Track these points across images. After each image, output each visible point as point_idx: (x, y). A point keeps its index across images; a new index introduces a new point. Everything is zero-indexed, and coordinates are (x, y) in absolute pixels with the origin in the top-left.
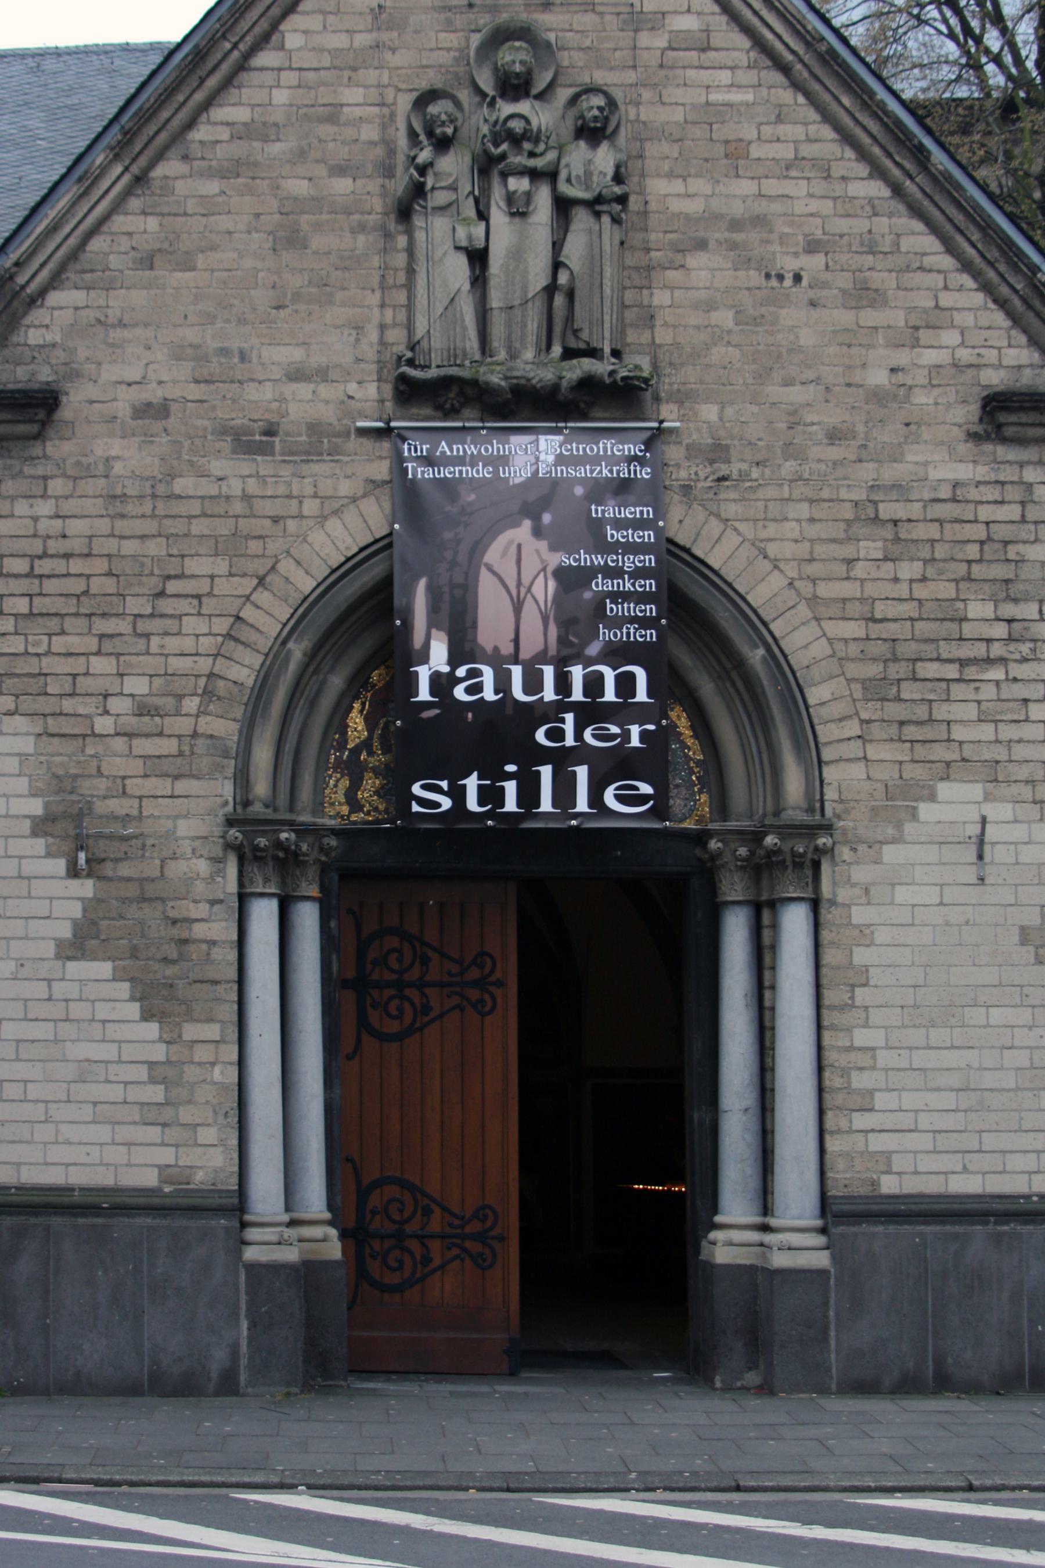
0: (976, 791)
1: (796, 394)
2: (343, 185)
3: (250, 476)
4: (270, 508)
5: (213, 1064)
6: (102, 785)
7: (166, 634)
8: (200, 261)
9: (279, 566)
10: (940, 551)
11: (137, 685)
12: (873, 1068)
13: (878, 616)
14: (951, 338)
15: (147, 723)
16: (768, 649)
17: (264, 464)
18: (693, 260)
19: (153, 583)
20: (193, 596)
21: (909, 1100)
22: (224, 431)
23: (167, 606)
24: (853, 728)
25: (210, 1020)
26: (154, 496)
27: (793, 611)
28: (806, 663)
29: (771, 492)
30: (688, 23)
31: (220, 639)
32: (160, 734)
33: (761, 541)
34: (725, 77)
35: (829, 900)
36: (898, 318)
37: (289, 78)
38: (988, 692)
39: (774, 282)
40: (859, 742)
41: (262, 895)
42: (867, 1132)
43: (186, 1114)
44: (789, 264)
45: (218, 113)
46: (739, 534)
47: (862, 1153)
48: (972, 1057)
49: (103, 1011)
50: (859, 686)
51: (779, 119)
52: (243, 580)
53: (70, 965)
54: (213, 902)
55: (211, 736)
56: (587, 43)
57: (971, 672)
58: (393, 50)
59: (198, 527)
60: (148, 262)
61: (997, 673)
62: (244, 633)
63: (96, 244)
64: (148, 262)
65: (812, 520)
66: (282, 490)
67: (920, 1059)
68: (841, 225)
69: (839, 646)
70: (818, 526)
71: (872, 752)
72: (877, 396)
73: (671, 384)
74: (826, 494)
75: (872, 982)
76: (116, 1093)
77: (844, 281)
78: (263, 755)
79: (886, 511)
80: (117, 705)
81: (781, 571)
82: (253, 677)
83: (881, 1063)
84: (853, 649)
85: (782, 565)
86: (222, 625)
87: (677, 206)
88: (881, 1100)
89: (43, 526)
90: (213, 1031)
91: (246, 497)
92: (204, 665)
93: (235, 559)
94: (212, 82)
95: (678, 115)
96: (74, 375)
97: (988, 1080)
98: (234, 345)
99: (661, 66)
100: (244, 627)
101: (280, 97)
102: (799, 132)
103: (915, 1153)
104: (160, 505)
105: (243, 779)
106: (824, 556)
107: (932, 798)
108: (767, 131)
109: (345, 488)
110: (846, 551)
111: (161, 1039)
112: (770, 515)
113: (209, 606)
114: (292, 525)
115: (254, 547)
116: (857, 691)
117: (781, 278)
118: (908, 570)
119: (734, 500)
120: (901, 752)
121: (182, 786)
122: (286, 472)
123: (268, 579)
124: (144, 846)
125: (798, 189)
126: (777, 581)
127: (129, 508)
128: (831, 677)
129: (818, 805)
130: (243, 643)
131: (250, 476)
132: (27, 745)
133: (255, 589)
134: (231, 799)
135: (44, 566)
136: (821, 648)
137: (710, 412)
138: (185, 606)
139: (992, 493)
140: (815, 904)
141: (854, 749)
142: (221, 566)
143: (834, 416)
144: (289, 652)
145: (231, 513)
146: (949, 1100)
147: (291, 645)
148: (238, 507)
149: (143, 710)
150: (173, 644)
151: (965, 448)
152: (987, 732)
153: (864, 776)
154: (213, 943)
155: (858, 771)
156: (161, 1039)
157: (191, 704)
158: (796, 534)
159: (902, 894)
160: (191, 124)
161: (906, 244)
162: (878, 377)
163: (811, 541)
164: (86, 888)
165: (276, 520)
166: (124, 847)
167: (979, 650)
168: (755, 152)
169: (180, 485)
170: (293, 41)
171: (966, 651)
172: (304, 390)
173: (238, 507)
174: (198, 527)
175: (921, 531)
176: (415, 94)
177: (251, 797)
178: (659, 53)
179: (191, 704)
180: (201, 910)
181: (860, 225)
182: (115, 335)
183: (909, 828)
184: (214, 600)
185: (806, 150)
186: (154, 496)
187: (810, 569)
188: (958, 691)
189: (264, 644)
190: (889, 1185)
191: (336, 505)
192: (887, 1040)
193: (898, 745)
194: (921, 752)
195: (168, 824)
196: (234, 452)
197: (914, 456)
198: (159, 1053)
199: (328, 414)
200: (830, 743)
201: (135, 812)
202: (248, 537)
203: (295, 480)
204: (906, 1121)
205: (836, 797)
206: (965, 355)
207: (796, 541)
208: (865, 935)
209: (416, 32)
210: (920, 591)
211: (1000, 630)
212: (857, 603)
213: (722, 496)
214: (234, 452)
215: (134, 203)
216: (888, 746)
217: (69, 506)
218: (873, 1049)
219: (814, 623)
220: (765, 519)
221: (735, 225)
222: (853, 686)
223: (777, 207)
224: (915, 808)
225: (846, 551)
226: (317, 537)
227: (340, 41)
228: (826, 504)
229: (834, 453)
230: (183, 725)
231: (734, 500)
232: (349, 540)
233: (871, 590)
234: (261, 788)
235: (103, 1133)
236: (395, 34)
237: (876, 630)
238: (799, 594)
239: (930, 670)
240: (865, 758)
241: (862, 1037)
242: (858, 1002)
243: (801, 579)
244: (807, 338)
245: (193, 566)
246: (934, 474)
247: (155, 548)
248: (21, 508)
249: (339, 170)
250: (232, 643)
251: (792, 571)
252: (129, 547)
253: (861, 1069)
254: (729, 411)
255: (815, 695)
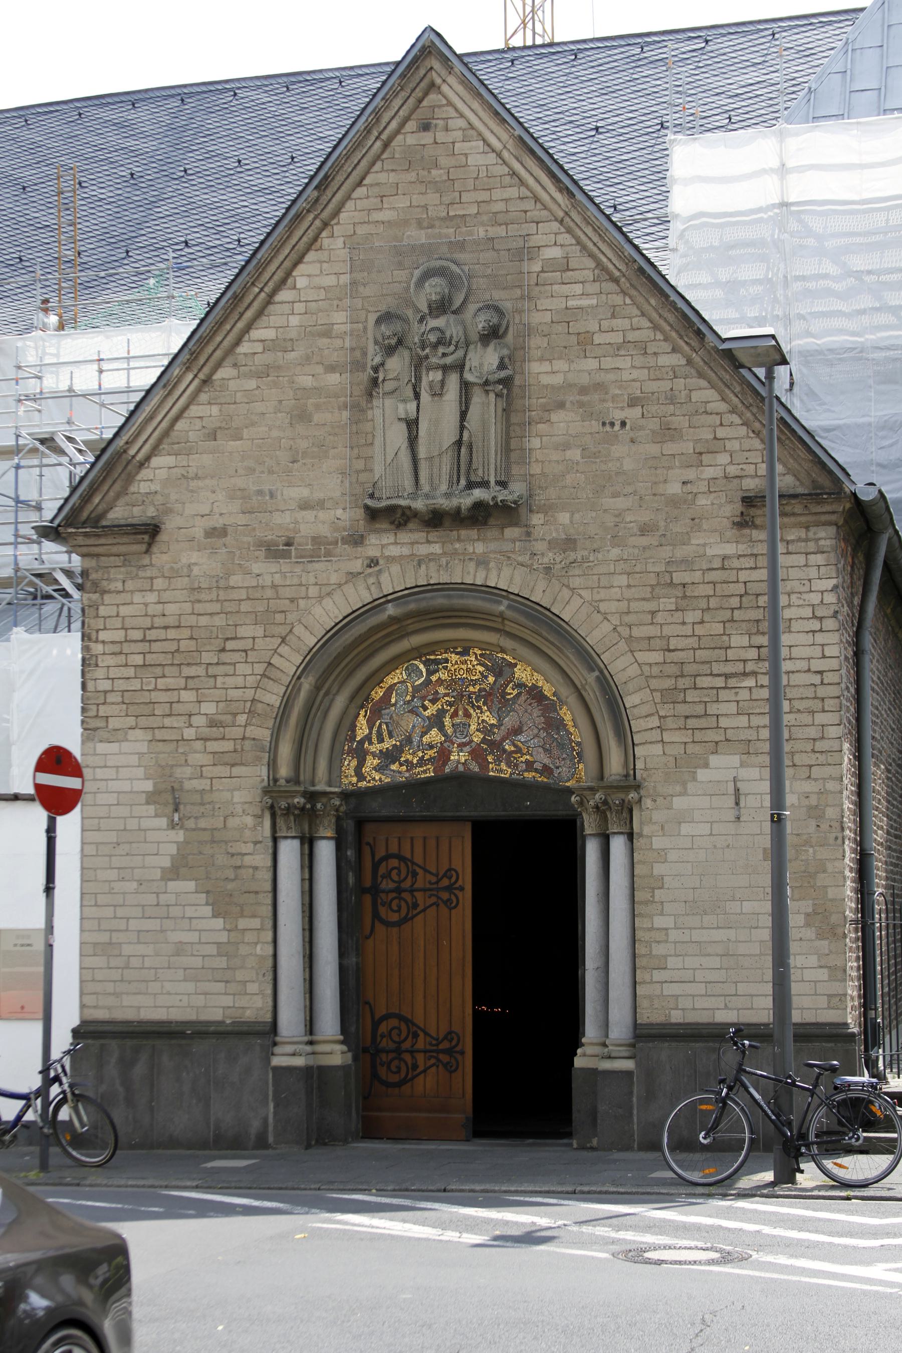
0: (735, 760)
1: (621, 503)
2: (334, 379)
3: (276, 573)
4: (287, 593)
5: (256, 944)
6: (188, 771)
7: (226, 675)
8: (245, 433)
9: (295, 630)
10: (713, 603)
11: (209, 708)
12: (666, 941)
13: (671, 647)
14: (723, 459)
15: (215, 732)
16: (601, 672)
17: (284, 565)
18: (554, 417)
19: (218, 643)
20: (242, 651)
21: (690, 962)
22: (260, 544)
23: (226, 657)
24: (654, 722)
25: (254, 916)
26: (218, 587)
27: (616, 647)
28: (624, 680)
29: (602, 569)
30: (555, 253)
31: (259, 677)
32: (223, 738)
33: (596, 601)
34: (578, 289)
35: (638, 833)
36: (688, 447)
37: (299, 307)
38: (744, 695)
39: (608, 428)
40: (659, 731)
41: (286, 838)
42: (662, 983)
43: (240, 975)
44: (618, 415)
45: (255, 334)
46: (581, 597)
47: (658, 996)
48: (731, 934)
49: (190, 912)
50: (659, 694)
51: (613, 316)
52: (272, 640)
53: (171, 884)
54: (256, 843)
55: (254, 739)
56: (489, 271)
57: (732, 682)
58: (364, 285)
59: (244, 607)
60: (213, 435)
62: (273, 673)
63: (179, 426)
64: (213, 435)
65: (629, 586)
66: (296, 581)
67: (697, 935)
68: (653, 386)
69: (646, 669)
70: (633, 589)
71: (667, 737)
72: (674, 502)
73: (539, 500)
74: (638, 569)
75: (666, 886)
76: (197, 962)
77: (654, 424)
78: (286, 750)
79: (678, 578)
80: (196, 720)
81: (609, 621)
82: (279, 701)
83: (671, 938)
84: (655, 670)
85: (609, 617)
86: (260, 669)
87: (546, 380)
88: (672, 962)
89: (151, 610)
90: (255, 923)
91: (274, 586)
92: (249, 693)
93: (267, 626)
94: (249, 314)
95: (547, 317)
96: (168, 511)
97: (742, 949)
98: (266, 488)
99: (537, 284)
100: (273, 669)
101: (294, 321)
102: (624, 323)
103: (693, 996)
104: (221, 593)
105: (273, 764)
106: (637, 610)
107: (706, 766)
108: (605, 324)
109: (334, 579)
111: (224, 929)
112: (602, 584)
113: (252, 656)
114: (302, 603)
115: (279, 617)
116: (657, 695)
117: (612, 424)
118: (692, 616)
119: (579, 576)
120: (685, 737)
121: (236, 771)
122: (298, 569)
123: (288, 638)
124: (214, 808)
125: (624, 363)
126: (606, 627)
127: (204, 596)
128: (640, 689)
129: (632, 772)
130: (272, 679)
131: (276, 573)
132: (143, 747)
133: (280, 645)
134: (266, 778)
135: (152, 635)
136: (634, 670)
137: (564, 518)
138: (237, 657)
139: (748, 562)
140: (630, 836)
141: (655, 735)
142: (259, 631)
143: (645, 517)
144: (301, 685)
145: (265, 597)
146: (715, 962)
147: (302, 680)
148: (269, 593)
149: (213, 723)
150: (230, 681)
151: (729, 534)
152: (743, 721)
153: (662, 753)
154: (256, 868)
155: (657, 749)
156: (224, 929)
157: (242, 719)
158: (619, 596)
159: (685, 829)
160: (238, 342)
161: (695, 396)
162: (674, 488)
163: (629, 600)
164: (179, 836)
165: (292, 600)
166: (202, 809)
167: (739, 667)
168: (598, 339)
169: (235, 580)
170: (301, 282)
171: (729, 668)
172: (309, 515)
173: (269, 593)
174: (244, 607)
176: (379, 314)
177: (278, 776)
178: (535, 275)
179: (242, 719)
180: (249, 848)
181: (665, 385)
182: (193, 484)
183: (690, 785)
184: (255, 652)
185: (632, 336)
186: (218, 587)
187: (627, 619)
188: (723, 695)
189: (286, 680)
190: (676, 1017)
191: (329, 589)
192: (675, 923)
193: (684, 732)
194: (699, 736)
195: (227, 795)
196: (266, 558)
197: (697, 539)
198: (223, 937)
199: (324, 530)
200: (639, 732)
201: (208, 788)
202: (275, 612)
203: (304, 574)
204: (688, 975)
205: (643, 767)
206: (732, 470)
207: (619, 600)
208: (662, 856)
209: (379, 272)
210: (699, 630)
212: (658, 640)
213: (570, 573)
214: (266, 558)
215: (203, 397)
216: (677, 732)
217: (166, 596)
218: (666, 929)
219: (629, 654)
220: (599, 587)
221: (584, 390)
222: (654, 694)
223: (611, 377)
224: (695, 772)
226: (318, 611)
227: (330, 281)
228: (639, 575)
229: (644, 541)
230: (237, 732)
231: (579, 576)
232: (336, 611)
233: (667, 631)
234: (284, 771)
235: (190, 987)
236: (366, 274)
237: (671, 656)
238: (620, 635)
239: (704, 682)
240: (662, 741)
241: (659, 922)
242: (657, 899)
243: (621, 625)
244: (628, 464)
245: (242, 631)
246: (710, 552)
247: (219, 621)
248: (137, 598)
249: (331, 369)
250: (266, 680)
251: (615, 620)
252: (204, 621)
253: (658, 942)
254: (577, 516)
255: (629, 701)
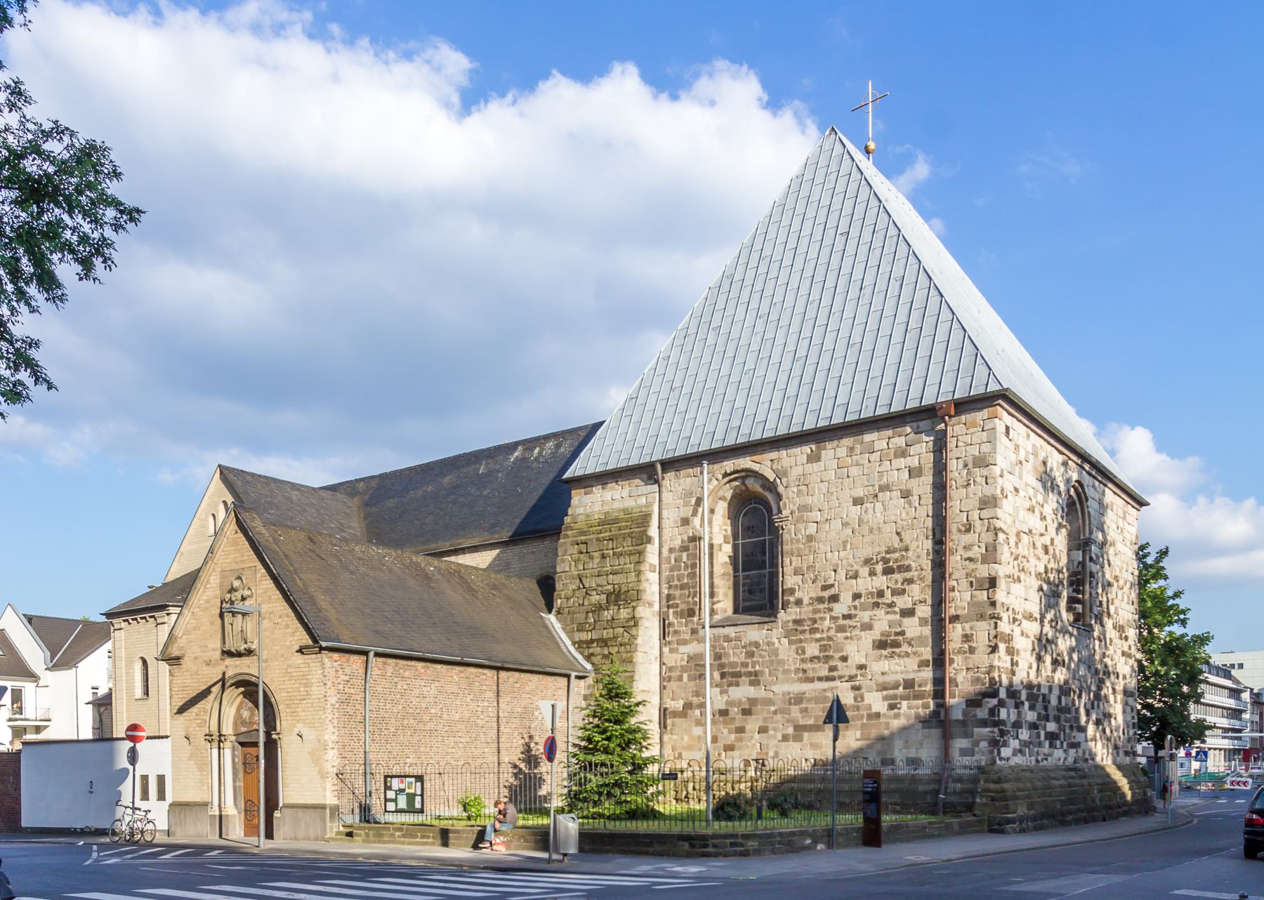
61: (304, 702)
79: (290, 670)
110: (283, 679)
118: (293, 682)
139: (304, 666)
152: (303, 714)
162: (288, 643)
175: (295, 674)
188: (300, 706)
211: (305, 693)
225: (283, 679)
239: (295, 702)
